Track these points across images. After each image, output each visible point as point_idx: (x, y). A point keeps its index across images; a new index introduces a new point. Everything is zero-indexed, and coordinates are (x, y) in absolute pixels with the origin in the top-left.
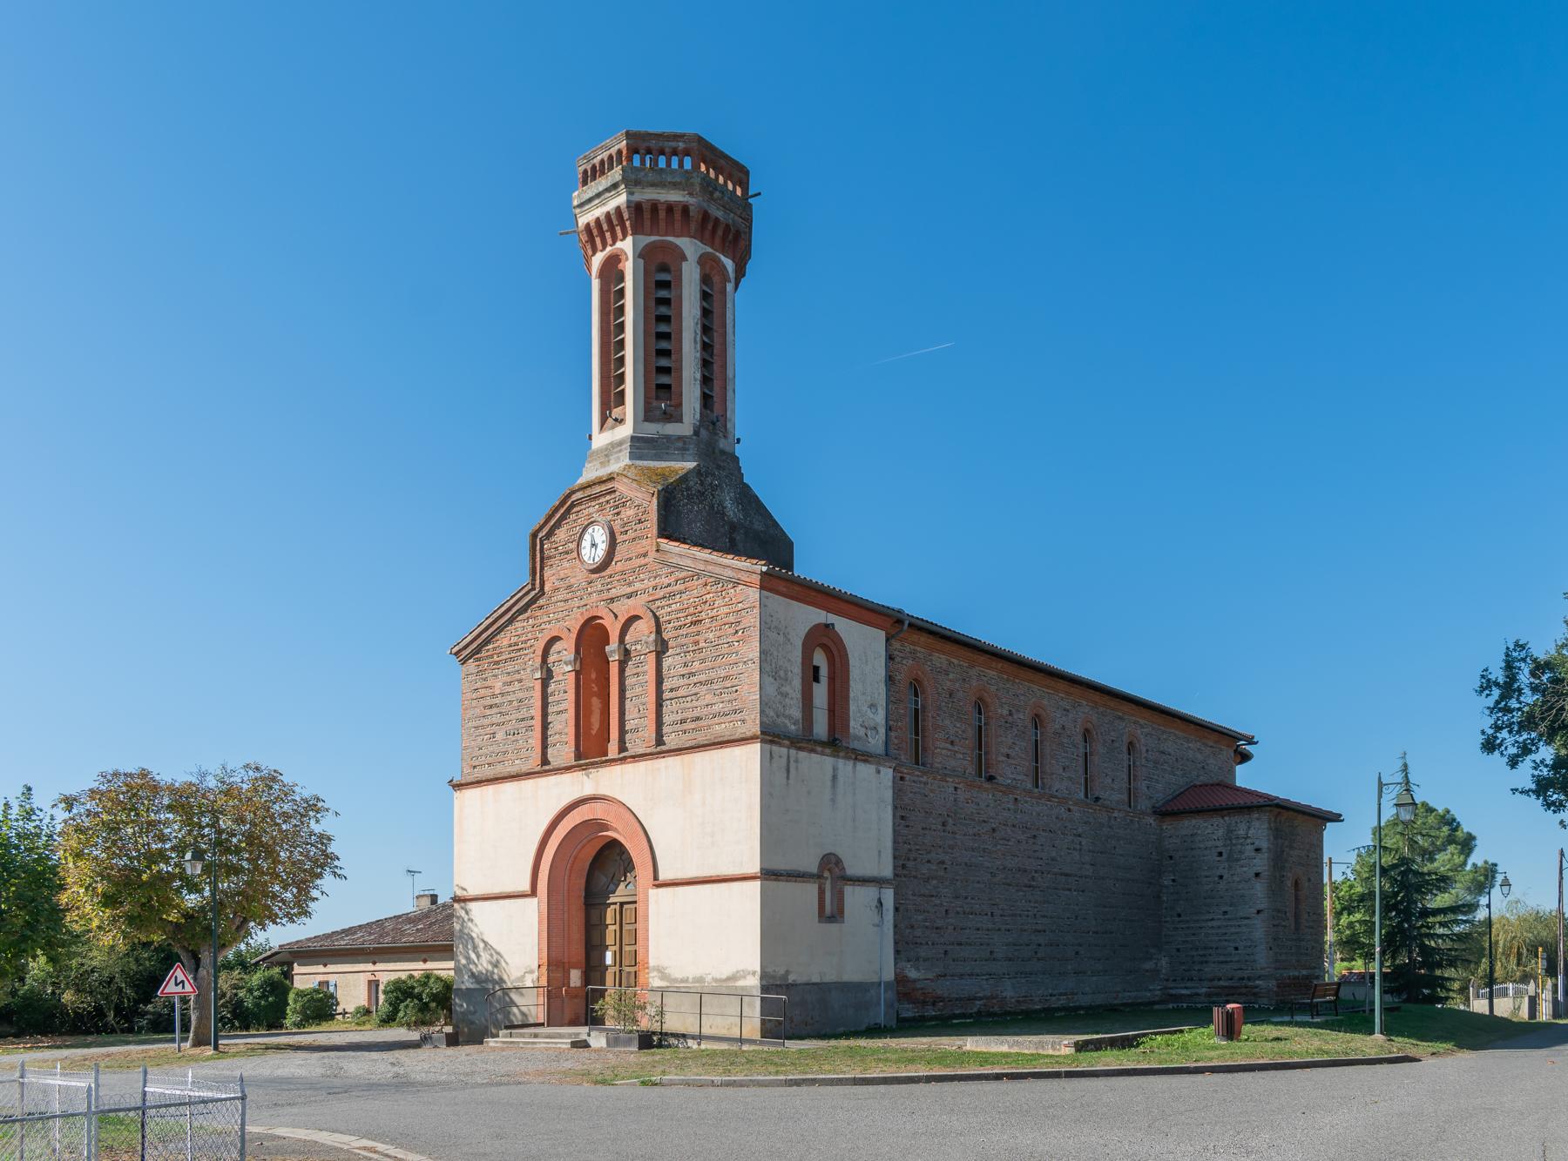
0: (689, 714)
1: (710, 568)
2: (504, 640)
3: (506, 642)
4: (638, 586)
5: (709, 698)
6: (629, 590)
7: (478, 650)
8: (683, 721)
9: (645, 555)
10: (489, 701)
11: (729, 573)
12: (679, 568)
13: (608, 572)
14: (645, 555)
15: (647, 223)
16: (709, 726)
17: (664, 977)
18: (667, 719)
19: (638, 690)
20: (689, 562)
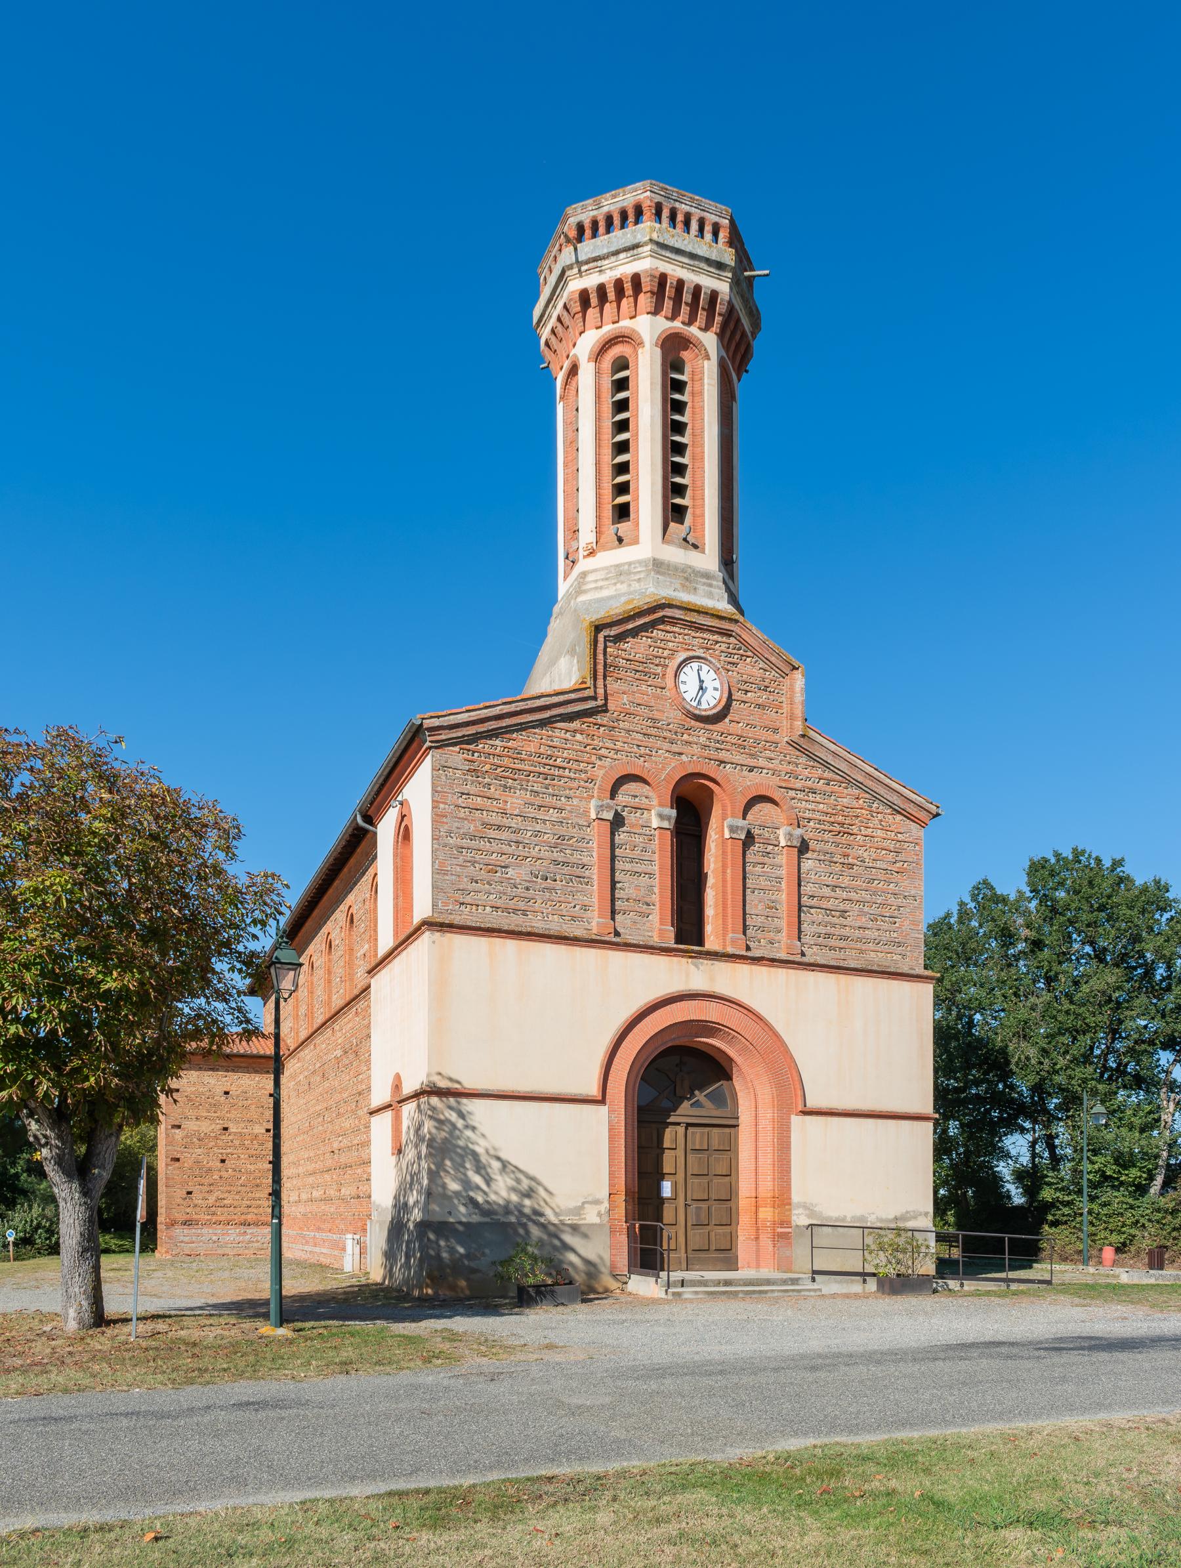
0: (837, 931)
1: (869, 783)
2: (530, 743)
3: (532, 748)
4: (762, 762)
5: (863, 921)
6: (753, 762)
7: (475, 739)
8: (828, 936)
9: (776, 730)
10: (495, 819)
11: (895, 799)
12: (826, 765)
13: (719, 727)
14: (776, 730)
15: (668, 304)
16: (861, 952)
17: (812, 1213)
18: (804, 927)
19: (764, 883)
20: (843, 766)
